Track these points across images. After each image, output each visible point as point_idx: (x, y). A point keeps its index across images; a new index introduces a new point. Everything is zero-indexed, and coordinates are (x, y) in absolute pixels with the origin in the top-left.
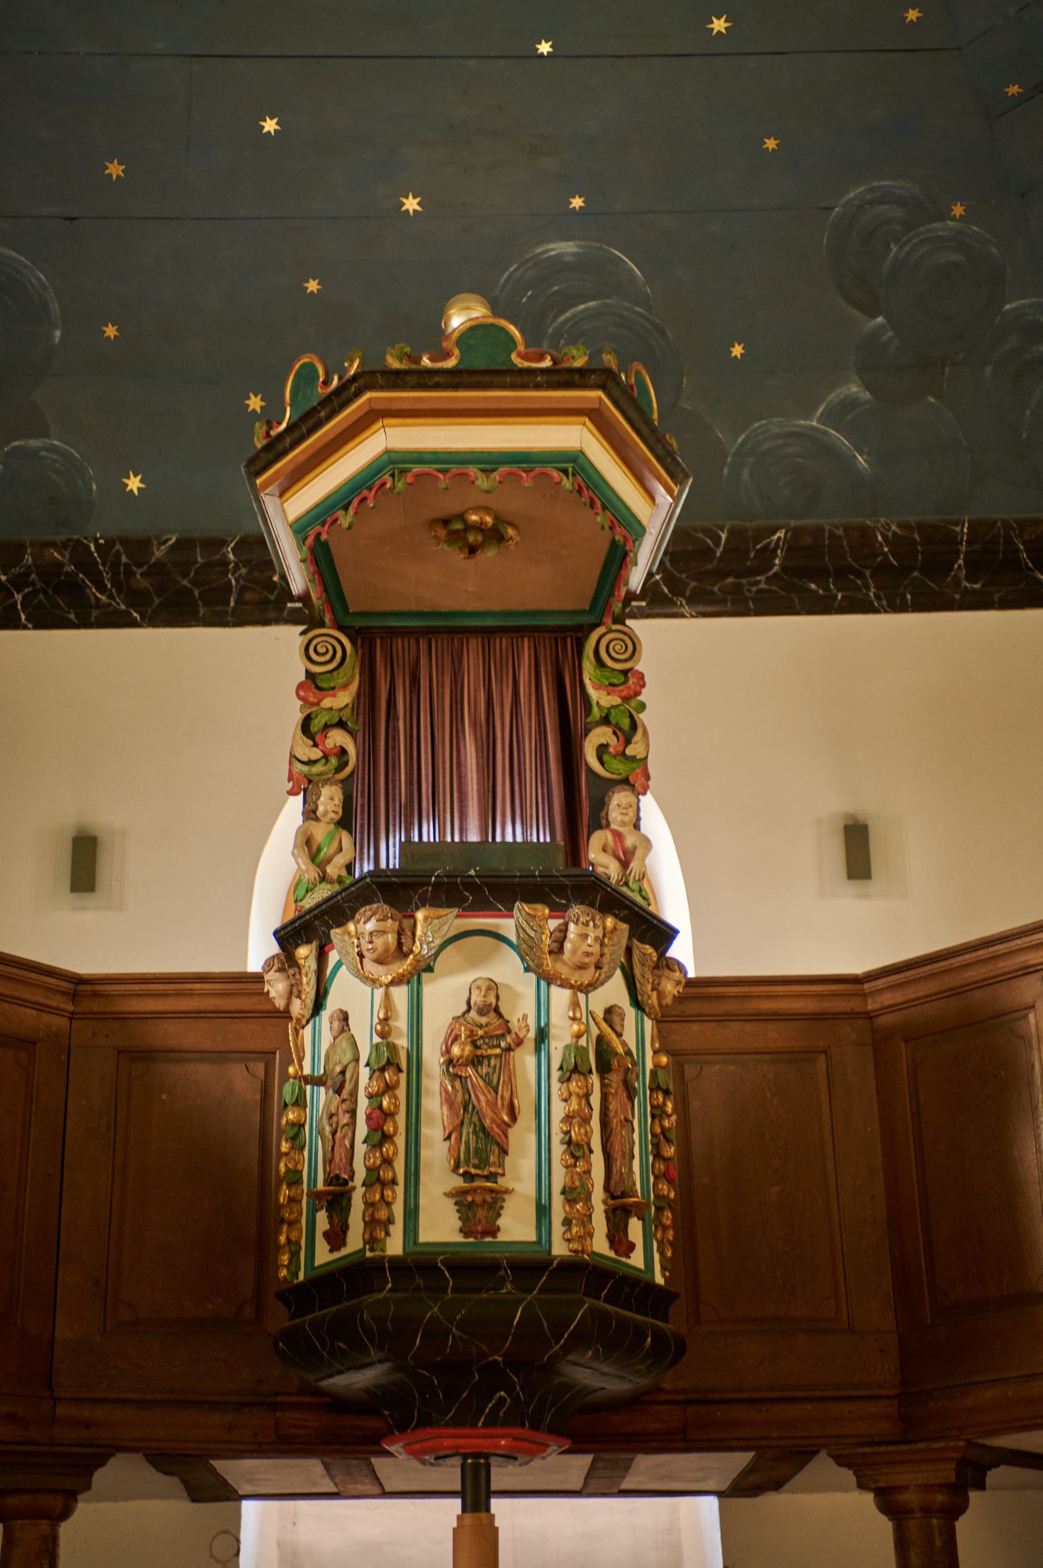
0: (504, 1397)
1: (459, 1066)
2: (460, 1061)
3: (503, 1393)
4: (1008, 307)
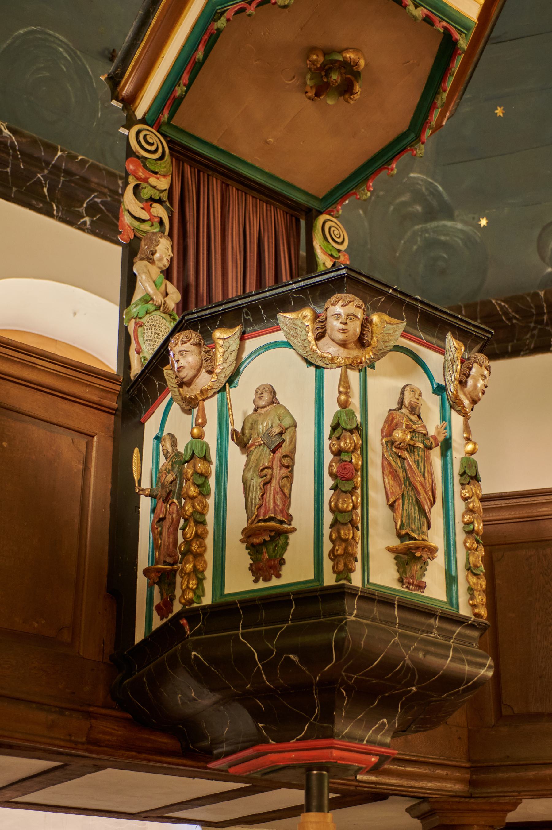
0: (385, 723)
1: (399, 448)
2: (402, 444)
3: (385, 720)
4: (412, 175)
